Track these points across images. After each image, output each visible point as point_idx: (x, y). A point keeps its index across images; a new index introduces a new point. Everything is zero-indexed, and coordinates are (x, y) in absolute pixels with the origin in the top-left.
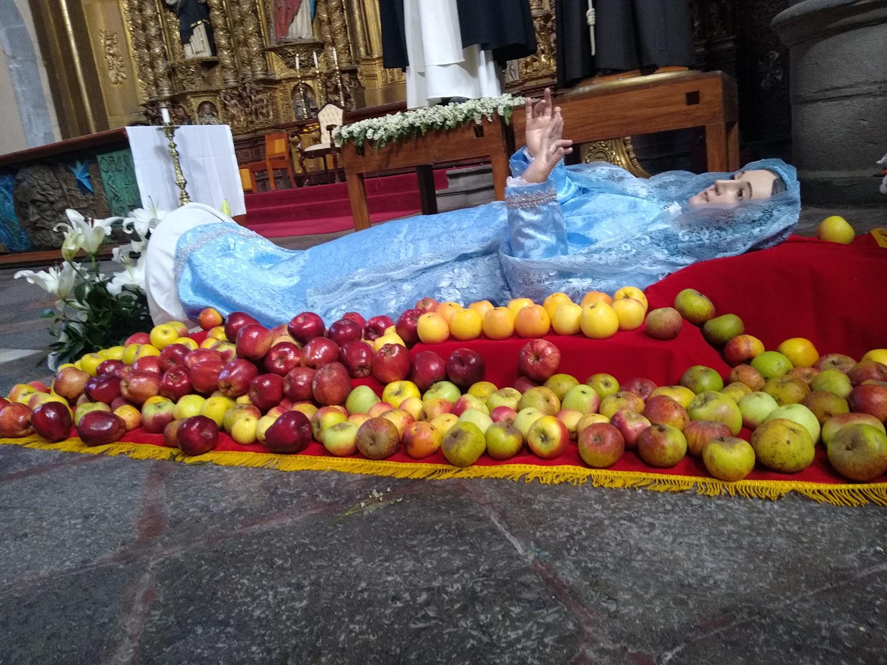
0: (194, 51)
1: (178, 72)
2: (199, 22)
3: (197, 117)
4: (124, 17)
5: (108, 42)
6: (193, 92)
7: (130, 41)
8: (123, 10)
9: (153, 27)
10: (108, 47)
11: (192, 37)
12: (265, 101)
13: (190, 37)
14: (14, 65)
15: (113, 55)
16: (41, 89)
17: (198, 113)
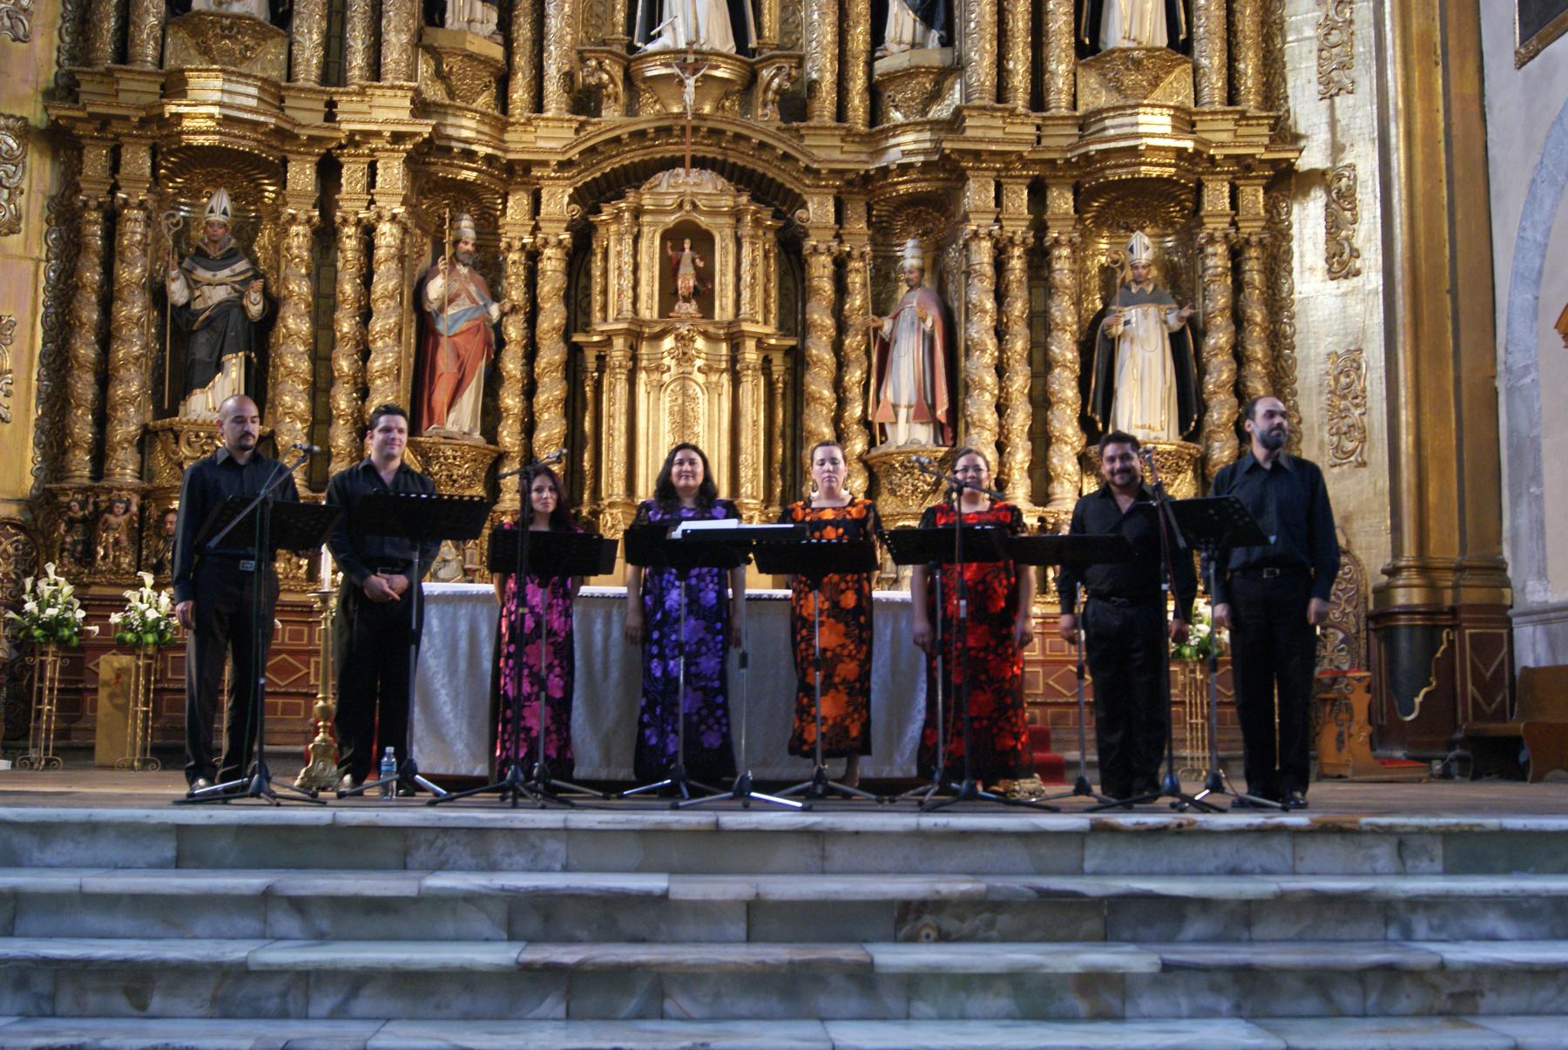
1: (182, 442)
13: (212, 378)
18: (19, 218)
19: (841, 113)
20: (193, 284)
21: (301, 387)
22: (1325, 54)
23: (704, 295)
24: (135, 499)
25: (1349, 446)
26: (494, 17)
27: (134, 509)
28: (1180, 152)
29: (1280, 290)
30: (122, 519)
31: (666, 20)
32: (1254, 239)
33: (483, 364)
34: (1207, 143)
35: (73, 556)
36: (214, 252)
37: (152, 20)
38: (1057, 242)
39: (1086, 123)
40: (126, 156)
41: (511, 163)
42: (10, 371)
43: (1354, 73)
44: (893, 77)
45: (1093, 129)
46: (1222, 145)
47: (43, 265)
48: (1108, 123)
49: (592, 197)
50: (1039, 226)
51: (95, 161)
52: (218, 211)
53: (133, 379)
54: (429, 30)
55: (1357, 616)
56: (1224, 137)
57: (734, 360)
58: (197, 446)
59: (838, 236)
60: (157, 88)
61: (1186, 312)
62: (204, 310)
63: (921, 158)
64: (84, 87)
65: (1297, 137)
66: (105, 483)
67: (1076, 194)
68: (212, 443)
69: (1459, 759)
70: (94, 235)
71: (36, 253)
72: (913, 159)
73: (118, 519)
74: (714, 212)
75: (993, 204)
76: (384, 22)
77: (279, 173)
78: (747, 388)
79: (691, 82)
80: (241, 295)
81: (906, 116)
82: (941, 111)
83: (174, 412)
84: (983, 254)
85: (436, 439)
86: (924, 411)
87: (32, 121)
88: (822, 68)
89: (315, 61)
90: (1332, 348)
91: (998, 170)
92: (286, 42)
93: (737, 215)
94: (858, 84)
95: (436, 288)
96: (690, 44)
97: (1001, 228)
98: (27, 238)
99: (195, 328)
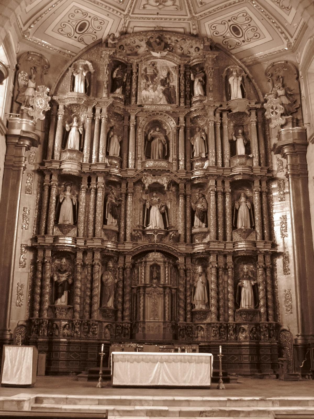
1: (56, 310)
18: (25, 264)
19: (185, 241)
20: (58, 277)
22: (282, 229)
23: (158, 278)
24: (47, 321)
25: (289, 309)
26: (116, 222)
27: (47, 323)
28: (253, 250)
29: (274, 277)
31: (150, 223)
32: (268, 267)
33: (113, 292)
34: (259, 249)
36: (62, 270)
37: (51, 225)
38: (229, 268)
39: (234, 244)
40: (47, 252)
41: (120, 252)
43: (287, 233)
44: (196, 233)
45: (236, 245)
46: (261, 249)
48: (239, 244)
49: (135, 258)
50: (226, 264)
51: (40, 254)
52: (64, 262)
54: (104, 225)
55: (291, 345)
56: (261, 247)
57: (164, 292)
59: (185, 266)
60: (53, 239)
61: (255, 282)
62: (60, 282)
63: (202, 251)
64: (39, 239)
65: (277, 245)
66: (42, 318)
67: (233, 257)
69: (311, 375)
72: (200, 251)
73: (44, 325)
74: (161, 262)
75: (216, 260)
76: (96, 225)
77: (75, 255)
78: (167, 297)
79: (156, 236)
81: (199, 241)
82: (206, 241)
83: (54, 304)
84: (214, 271)
85: (105, 308)
86: (203, 302)
87: (28, 245)
88: (181, 232)
89: (82, 232)
90: (285, 289)
91: (217, 254)
92: (77, 228)
93: (165, 262)
94: (188, 234)
95: (105, 277)
96: (155, 227)
97: (218, 265)
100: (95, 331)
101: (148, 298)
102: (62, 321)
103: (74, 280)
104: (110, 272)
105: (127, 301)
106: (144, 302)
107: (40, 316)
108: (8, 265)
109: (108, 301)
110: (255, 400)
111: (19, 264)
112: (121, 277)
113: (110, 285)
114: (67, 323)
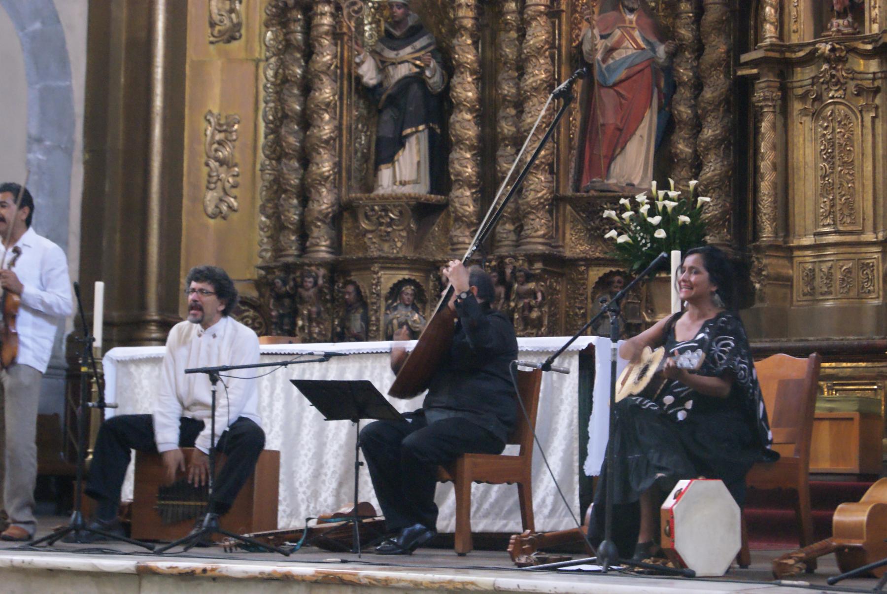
0: (398, 179)
1: (361, 216)
2: (421, 128)
3: (383, 309)
4: (262, 94)
5: (219, 137)
6: (387, 258)
7: (262, 140)
8: (262, 81)
9: (328, 123)
10: (215, 146)
11: (400, 153)
12: (539, 295)
13: (395, 152)
14: (38, 156)
15: (222, 162)
16: (68, 206)
17: (387, 299)
18: (237, 26)
20: (383, 66)
21: (468, 155)
24: (322, 272)
30: (311, 292)
35: (282, 329)
36: (397, 33)
42: (236, 165)
47: (262, 65)
53: (322, 162)
58: (374, 218)
68: (387, 215)
70: (296, 32)
71: (257, 55)
73: (309, 293)
80: (422, 69)
98: (247, 41)
99: (380, 106)
100: (531, 308)
101: (807, 120)
102: (376, 267)
103: (450, 68)
104: (632, 11)
105: (707, 149)
106: (784, 148)
107: (303, 250)
108: (143, 34)
109: (612, 158)
110: (287, 579)
111: (209, 31)
112: (686, 33)
113: (621, 74)
114: (404, 275)
